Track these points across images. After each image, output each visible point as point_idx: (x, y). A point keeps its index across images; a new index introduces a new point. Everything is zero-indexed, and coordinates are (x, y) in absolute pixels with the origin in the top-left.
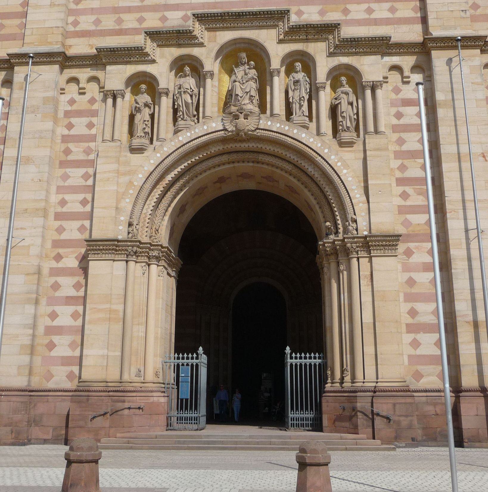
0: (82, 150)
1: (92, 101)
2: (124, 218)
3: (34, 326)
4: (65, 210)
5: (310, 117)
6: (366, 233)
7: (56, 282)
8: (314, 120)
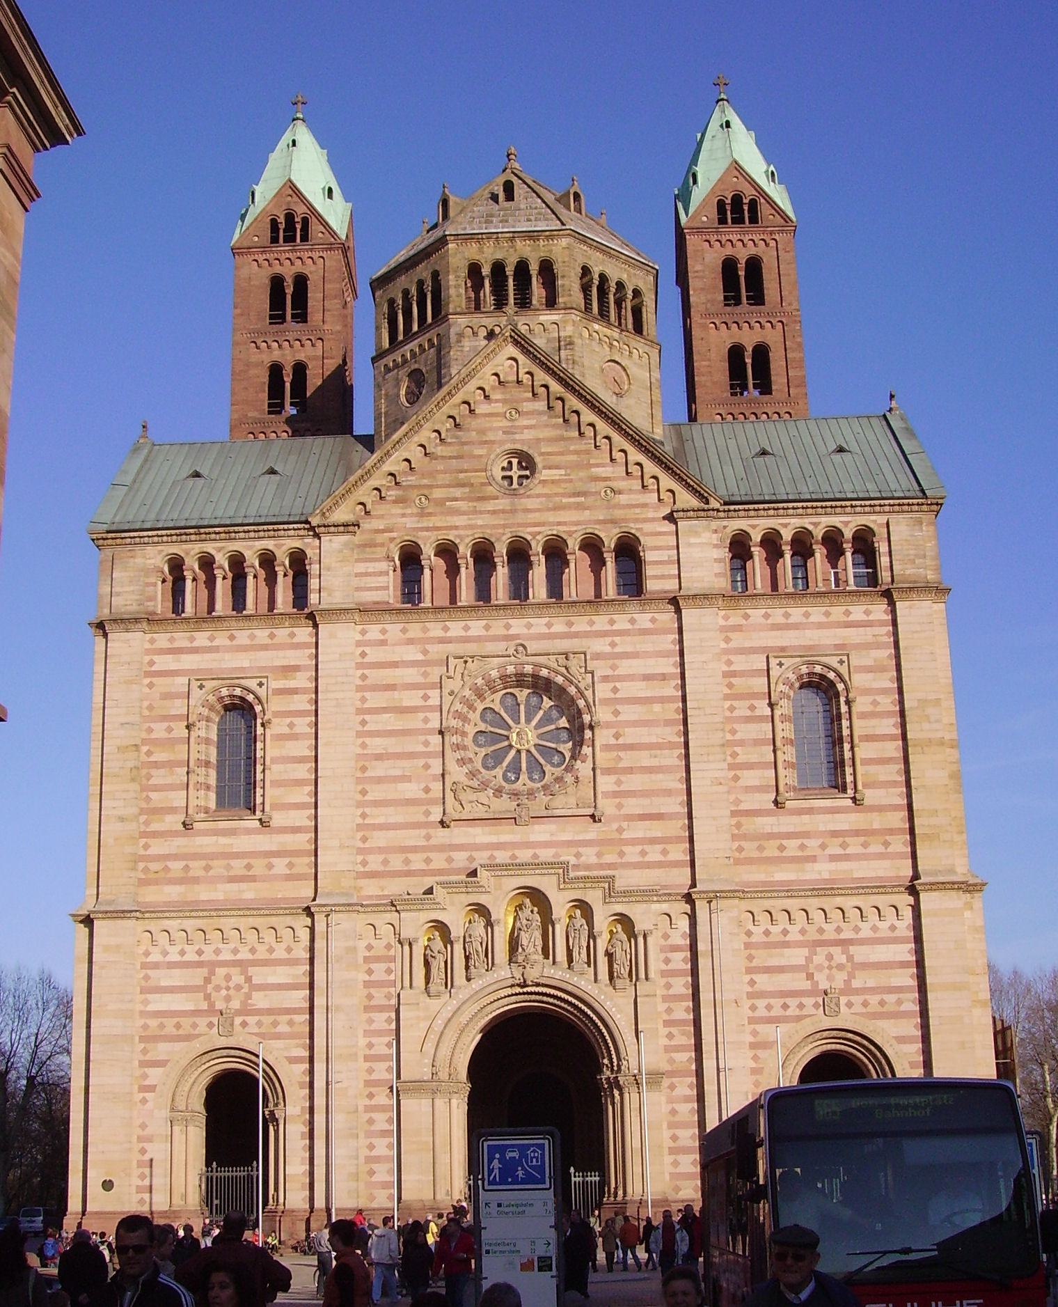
0: (383, 995)
1: (389, 947)
2: (428, 1061)
3: (357, 1158)
4: (372, 1052)
5: (589, 966)
6: (636, 1071)
7: (371, 1117)
8: (592, 965)
